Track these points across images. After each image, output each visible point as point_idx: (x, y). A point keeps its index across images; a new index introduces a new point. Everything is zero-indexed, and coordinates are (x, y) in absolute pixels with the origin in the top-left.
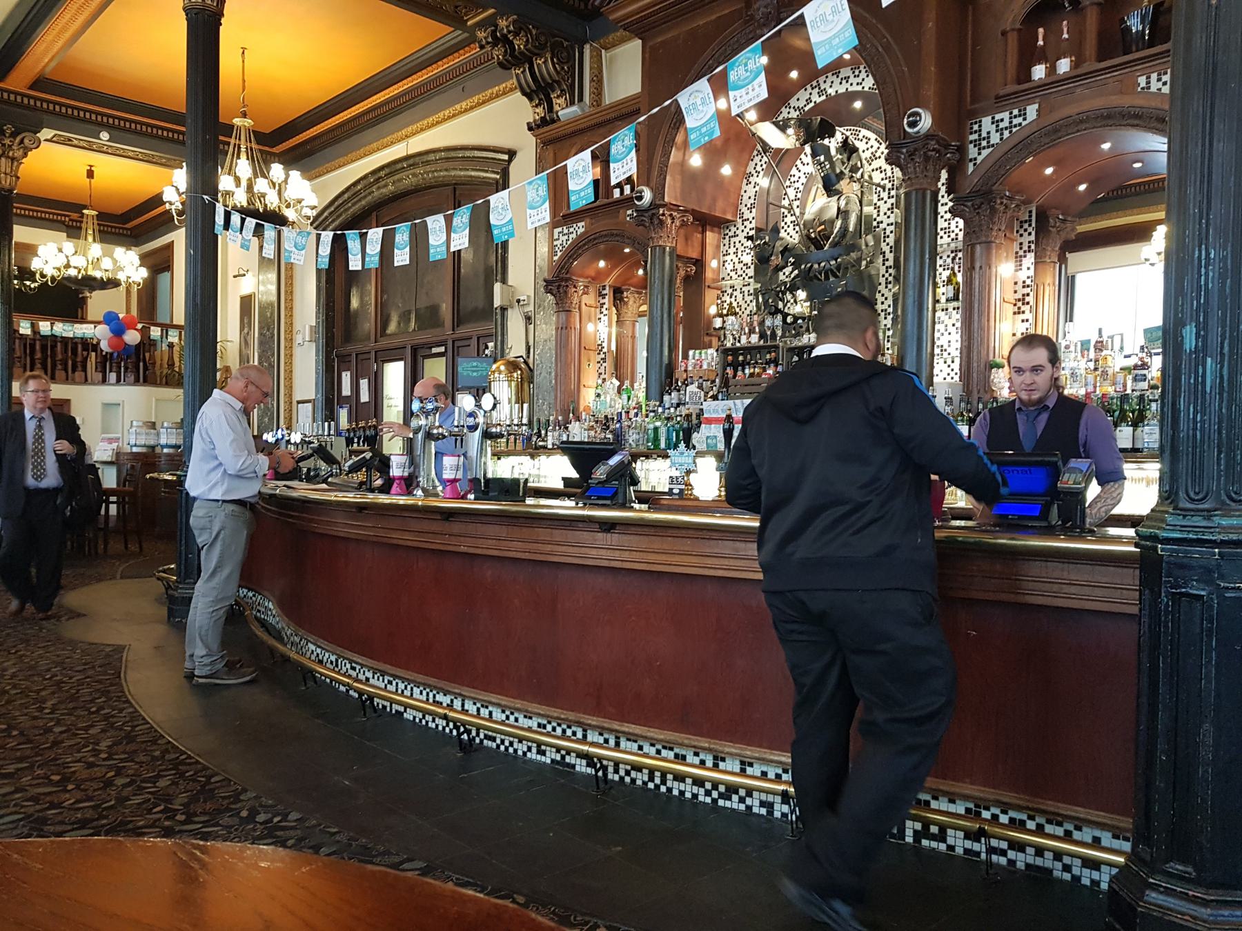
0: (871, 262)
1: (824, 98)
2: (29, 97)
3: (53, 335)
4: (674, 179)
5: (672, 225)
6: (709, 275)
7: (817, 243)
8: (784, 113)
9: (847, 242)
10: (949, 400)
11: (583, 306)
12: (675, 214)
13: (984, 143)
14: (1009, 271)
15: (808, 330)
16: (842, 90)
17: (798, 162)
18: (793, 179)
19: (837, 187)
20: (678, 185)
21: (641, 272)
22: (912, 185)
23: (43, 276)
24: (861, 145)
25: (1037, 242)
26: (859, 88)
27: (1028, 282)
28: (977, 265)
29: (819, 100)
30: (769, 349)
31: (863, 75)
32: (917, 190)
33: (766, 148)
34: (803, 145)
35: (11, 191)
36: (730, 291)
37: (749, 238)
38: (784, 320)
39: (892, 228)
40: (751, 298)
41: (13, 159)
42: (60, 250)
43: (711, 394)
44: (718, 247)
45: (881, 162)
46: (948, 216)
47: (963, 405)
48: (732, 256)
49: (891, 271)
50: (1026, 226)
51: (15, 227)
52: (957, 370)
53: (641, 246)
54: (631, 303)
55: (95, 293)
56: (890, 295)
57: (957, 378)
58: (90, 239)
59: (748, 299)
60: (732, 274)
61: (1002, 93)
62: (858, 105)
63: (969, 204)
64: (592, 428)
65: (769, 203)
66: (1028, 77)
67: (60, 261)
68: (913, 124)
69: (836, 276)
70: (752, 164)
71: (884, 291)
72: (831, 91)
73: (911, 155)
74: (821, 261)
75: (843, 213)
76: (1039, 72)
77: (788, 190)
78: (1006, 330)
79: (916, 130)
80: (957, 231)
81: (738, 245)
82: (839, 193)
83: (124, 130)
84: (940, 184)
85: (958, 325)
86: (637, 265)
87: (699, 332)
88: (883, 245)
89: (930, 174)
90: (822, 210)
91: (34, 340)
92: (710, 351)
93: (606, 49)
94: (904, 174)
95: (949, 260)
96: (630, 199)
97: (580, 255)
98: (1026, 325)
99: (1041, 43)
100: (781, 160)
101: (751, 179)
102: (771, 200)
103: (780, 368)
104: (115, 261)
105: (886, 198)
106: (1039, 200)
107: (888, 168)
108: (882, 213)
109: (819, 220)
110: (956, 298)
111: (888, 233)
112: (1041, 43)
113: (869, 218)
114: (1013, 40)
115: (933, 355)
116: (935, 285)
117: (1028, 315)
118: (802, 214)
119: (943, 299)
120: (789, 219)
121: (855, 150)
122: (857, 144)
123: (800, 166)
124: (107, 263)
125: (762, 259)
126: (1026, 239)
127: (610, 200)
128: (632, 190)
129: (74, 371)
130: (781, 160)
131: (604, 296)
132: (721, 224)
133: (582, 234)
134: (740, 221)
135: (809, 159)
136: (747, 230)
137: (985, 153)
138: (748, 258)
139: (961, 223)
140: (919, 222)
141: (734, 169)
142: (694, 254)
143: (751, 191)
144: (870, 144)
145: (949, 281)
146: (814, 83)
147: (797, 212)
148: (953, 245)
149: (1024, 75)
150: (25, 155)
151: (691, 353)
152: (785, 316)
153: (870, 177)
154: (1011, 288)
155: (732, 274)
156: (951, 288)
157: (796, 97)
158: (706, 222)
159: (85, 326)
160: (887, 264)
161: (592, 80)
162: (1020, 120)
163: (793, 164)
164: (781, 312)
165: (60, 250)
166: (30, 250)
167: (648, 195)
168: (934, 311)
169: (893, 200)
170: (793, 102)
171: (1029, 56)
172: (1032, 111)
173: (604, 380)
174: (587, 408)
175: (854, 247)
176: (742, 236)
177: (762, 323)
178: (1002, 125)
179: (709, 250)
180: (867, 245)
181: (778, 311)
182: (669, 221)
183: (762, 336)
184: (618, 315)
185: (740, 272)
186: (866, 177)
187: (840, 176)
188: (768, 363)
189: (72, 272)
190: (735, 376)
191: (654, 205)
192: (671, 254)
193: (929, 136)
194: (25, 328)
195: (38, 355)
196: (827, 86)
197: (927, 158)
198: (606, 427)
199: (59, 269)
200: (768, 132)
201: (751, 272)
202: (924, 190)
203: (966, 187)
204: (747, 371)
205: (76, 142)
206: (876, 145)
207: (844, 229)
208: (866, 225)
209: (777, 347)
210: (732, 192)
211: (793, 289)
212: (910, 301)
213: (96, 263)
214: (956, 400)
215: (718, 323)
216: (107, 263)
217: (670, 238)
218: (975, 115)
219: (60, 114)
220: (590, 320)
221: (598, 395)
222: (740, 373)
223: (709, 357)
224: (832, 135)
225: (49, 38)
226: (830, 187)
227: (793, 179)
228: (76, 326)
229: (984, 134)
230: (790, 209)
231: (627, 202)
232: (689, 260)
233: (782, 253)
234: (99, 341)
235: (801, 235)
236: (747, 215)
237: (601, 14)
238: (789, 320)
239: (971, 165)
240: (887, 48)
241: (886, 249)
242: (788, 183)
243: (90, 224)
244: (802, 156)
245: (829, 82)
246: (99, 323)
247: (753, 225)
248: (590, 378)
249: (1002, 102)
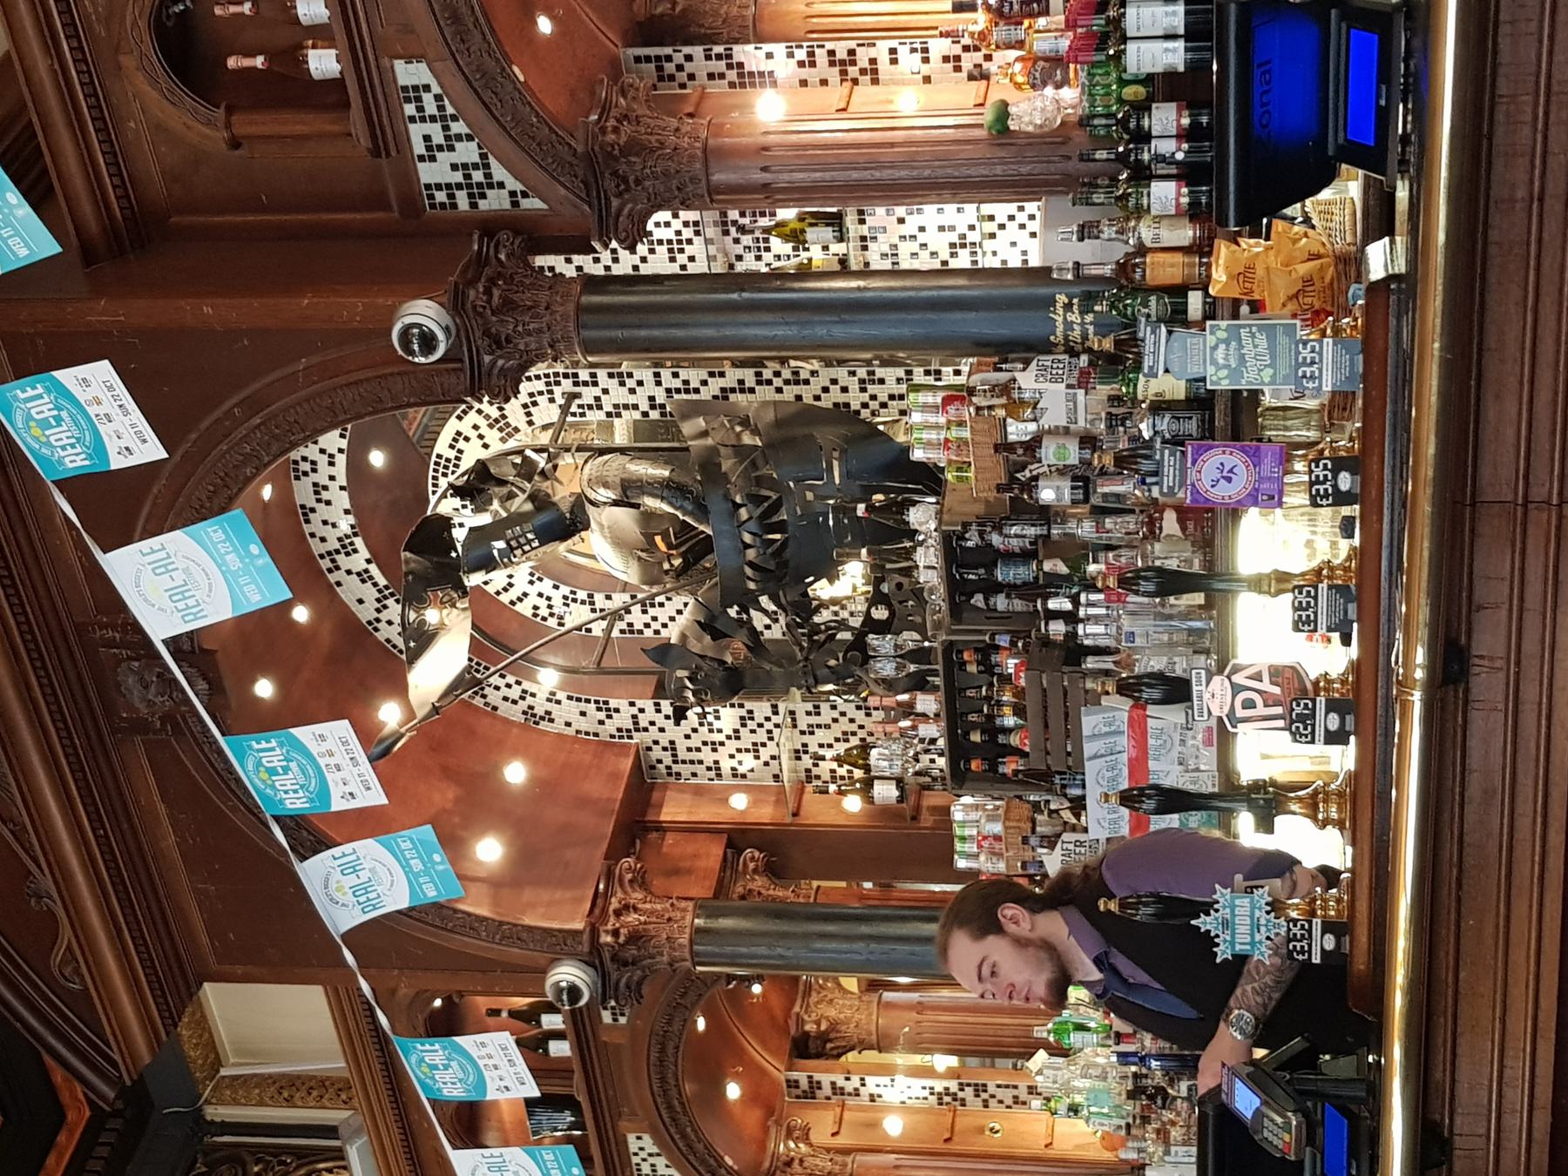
0: (745, 422)
1: (359, 542)
4: (532, 906)
5: (640, 911)
6: (766, 814)
7: (695, 551)
8: (389, 633)
9: (697, 482)
10: (1086, 231)
11: (840, 1141)
12: (615, 904)
13: (478, 176)
14: (775, 102)
15: (908, 572)
16: (343, 500)
17: (505, 598)
18: (544, 612)
19: (565, 507)
20: (545, 895)
21: (757, 989)
22: (567, 339)
24: (472, 454)
25: (707, 39)
26: (341, 460)
27: (801, 54)
28: (759, 177)
29: (364, 553)
30: (953, 664)
31: (311, 451)
32: (579, 326)
33: (468, 682)
34: (464, 592)
36: (807, 761)
37: (679, 715)
38: (881, 628)
39: (666, 374)
40: (825, 707)
43: (1067, 816)
44: (699, 791)
45: (514, 409)
46: (642, 249)
47: (1098, 198)
48: (722, 755)
49: (767, 374)
50: (670, 68)
52: (1012, 208)
53: (690, 990)
54: (832, 1013)
56: (826, 374)
57: (1031, 207)
59: (827, 714)
60: (765, 754)
61: (365, 142)
62: (377, 458)
63: (615, 203)
64: (1163, 1135)
65: (597, 668)
66: (337, 84)
68: (428, 342)
69: (776, 507)
70: (505, 710)
71: (816, 386)
72: (345, 524)
73: (497, 343)
74: (738, 540)
75: (629, 492)
76: (323, 63)
77: (570, 622)
78: (918, 99)
79: (441, 336)
80: (677, 224)
81: (695, 741)
82: (580, 502)
84: (570, 272)
85: (900, 211)
86: (738, 997)
87: (911, 839)
88: (706, 394)
89: (543, 297)
90: (619, 542)
92: (958, 815)
93: (218, 1063)
94: (541, 357)
95: (747, 240)
96: (575, 1017)
97: (709, 1147)
98: (903, 52)
99: (259, 61)
100: (499, 640)
101: (539, 711)
102: (588, 662)
103: (1003, 640)
105: (597, 391)
106: (610, 39)
107: (525, 387)
108: (632, 400)
109: (643, 549)
110: (836, 221)
111: (677, 383)
112: (259, 61)
113: (638, 429)
114: (249, 124)
115: (974, 273)
116: (805, 272)
117: (881, 50)
118: (625, 587)
119: (838, 248)
120: (637, 617)
121: (481, 468)
122: (467, 463)
123: (513, 594)
125: (730, 684)
126: (700, 66)
127: (576, 1066)
128: (551, 1008)
130: (499, 640)
131: (815, 1086)
132: (644, 782)
133: (658, 1141)
134: (637, 738)
135: (498, 578)
136: (660, 720)
137: (499, 172)
138: (728, 717)
139: (663, 216)
140: (653, 318)
141: (516, 753)
142: (714, 852)
143: (567, 711)
144: (469, 436)
145: (797, 238)
146: (325, 564)
147: (620, 599)
148: (711, 232)
149: (331, 93)
151: (961, 864)
152: (871, 625)
153: (545, 427)
154: (815, 95)
155: (765, 754)
156: (811, 234)
157: (355, 607)
158: (636, 824)
160: (750, 381)
161: (290, 1102)
162: (428, 99)
163: (508, 610)
164: (860, 635)
167: (567, 973)
168: (866, 272)
169: (602, 374)
170: (365, 613)
171: (287, 85)
172: (409, 73)
173: (1032, 1090)
174: (1108, 1141)
175: (709, 464)
176: (674, 732)
177: (890, 685)
178: (439, 139)
179: (706, 813)
180: (704, 434)
181: (859, 643)
182: (632, 918)
183: (919, 683)
184: (863, 1046)
185: (761, 736)
186: (545, 438)
187: (541, 501)
188: (988, 668)
190: (1025, 755)
191: (593, 958)
192: (712, 914)
193: (456, 305)
196: (332, 535)
197: (508, 306)
198: (1160, 1096)
200: (432, 675)
201: (761, 709)
202: (580, 309)
203: (580, 213)
204: (1010, 721)
206: (472, 417)
207: (666, 489)
208: (657, 435)
209: (949, 647)
210: (565, 759)
211: (804, 608)
212: (839, 332)
214: (1085, 214)
215: (885, 792)
217: (673, 918)
218: (412, 197)
220: (875, 1125)
221: (1074, 1110)
222: (1014, 740)
223: (972, 816)
224: (445, 523)
226: (569, 524)
227: (544, 612)
229: (458, 177)
230: (616, 615)
231: (582, 1026)
232: (729, 865)
233: (717, 635)
235: (676, 590)
236: (623, 720)
237: (140, 1082)
238: (880, 613)
239: (526, 204)
240: (253, 405)
241: (715, 385)
242: (552, 622)
244: (491, 589)
245: (327, 531)
247: (648, 705)
248: (1029, 1128)
249: (386, 141)
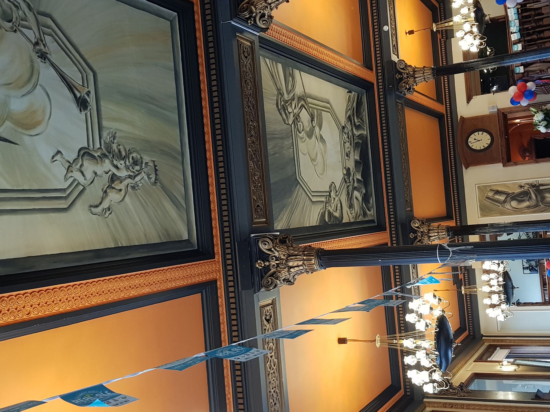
2: (377, 70)
3: (520, 31)
23: (481, 44)
35: (433, 69)
41: (414, 71)
42: (462, 38)
51: (454, 63)
55: (486, 12)
58: (451, 23)
67: (469, 38)
83: (379, 18)
91: (525, 41)
104: (462, 6)
124: (465, 11)
129: (543, 14)
150: (410, 66)
159: (509, 14)
165: (462, 38)
166: (467, 54)
189: (475, 29)
194: (518, 47)
195: (535, 37)
199: (475, 36)
205: (394, 43)
213: (466, 17)
216: (465, 11)
219: (381, 53)
225: (342, 65)
228: (510, 19)
234: (518, 4)
243: (443, 25)
246: (505, 7)
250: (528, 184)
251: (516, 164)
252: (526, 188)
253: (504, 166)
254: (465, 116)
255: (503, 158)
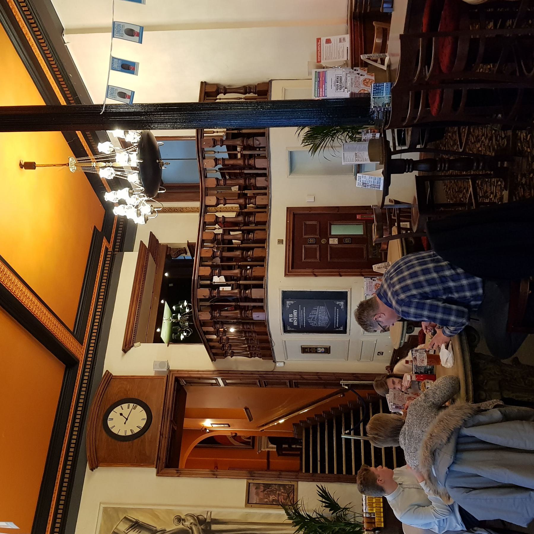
250: (192, 516)
251: (179, 474)
252: (187, 523)
253: (158, 474)
254: (114, 374)
255: (159, 458)
